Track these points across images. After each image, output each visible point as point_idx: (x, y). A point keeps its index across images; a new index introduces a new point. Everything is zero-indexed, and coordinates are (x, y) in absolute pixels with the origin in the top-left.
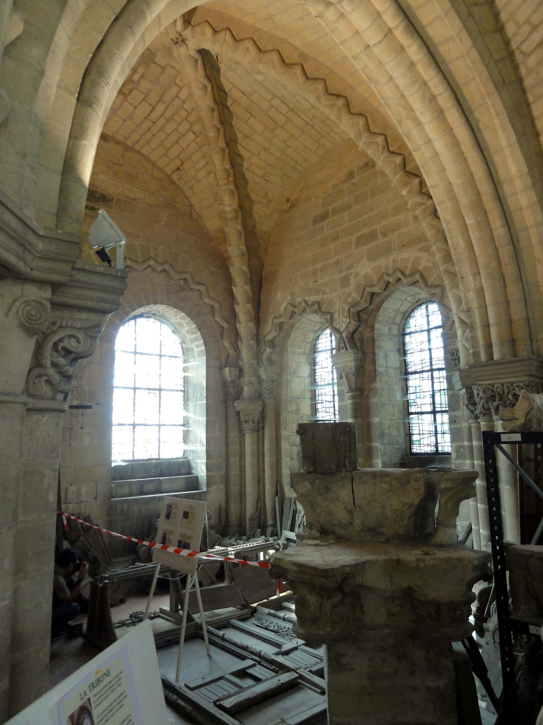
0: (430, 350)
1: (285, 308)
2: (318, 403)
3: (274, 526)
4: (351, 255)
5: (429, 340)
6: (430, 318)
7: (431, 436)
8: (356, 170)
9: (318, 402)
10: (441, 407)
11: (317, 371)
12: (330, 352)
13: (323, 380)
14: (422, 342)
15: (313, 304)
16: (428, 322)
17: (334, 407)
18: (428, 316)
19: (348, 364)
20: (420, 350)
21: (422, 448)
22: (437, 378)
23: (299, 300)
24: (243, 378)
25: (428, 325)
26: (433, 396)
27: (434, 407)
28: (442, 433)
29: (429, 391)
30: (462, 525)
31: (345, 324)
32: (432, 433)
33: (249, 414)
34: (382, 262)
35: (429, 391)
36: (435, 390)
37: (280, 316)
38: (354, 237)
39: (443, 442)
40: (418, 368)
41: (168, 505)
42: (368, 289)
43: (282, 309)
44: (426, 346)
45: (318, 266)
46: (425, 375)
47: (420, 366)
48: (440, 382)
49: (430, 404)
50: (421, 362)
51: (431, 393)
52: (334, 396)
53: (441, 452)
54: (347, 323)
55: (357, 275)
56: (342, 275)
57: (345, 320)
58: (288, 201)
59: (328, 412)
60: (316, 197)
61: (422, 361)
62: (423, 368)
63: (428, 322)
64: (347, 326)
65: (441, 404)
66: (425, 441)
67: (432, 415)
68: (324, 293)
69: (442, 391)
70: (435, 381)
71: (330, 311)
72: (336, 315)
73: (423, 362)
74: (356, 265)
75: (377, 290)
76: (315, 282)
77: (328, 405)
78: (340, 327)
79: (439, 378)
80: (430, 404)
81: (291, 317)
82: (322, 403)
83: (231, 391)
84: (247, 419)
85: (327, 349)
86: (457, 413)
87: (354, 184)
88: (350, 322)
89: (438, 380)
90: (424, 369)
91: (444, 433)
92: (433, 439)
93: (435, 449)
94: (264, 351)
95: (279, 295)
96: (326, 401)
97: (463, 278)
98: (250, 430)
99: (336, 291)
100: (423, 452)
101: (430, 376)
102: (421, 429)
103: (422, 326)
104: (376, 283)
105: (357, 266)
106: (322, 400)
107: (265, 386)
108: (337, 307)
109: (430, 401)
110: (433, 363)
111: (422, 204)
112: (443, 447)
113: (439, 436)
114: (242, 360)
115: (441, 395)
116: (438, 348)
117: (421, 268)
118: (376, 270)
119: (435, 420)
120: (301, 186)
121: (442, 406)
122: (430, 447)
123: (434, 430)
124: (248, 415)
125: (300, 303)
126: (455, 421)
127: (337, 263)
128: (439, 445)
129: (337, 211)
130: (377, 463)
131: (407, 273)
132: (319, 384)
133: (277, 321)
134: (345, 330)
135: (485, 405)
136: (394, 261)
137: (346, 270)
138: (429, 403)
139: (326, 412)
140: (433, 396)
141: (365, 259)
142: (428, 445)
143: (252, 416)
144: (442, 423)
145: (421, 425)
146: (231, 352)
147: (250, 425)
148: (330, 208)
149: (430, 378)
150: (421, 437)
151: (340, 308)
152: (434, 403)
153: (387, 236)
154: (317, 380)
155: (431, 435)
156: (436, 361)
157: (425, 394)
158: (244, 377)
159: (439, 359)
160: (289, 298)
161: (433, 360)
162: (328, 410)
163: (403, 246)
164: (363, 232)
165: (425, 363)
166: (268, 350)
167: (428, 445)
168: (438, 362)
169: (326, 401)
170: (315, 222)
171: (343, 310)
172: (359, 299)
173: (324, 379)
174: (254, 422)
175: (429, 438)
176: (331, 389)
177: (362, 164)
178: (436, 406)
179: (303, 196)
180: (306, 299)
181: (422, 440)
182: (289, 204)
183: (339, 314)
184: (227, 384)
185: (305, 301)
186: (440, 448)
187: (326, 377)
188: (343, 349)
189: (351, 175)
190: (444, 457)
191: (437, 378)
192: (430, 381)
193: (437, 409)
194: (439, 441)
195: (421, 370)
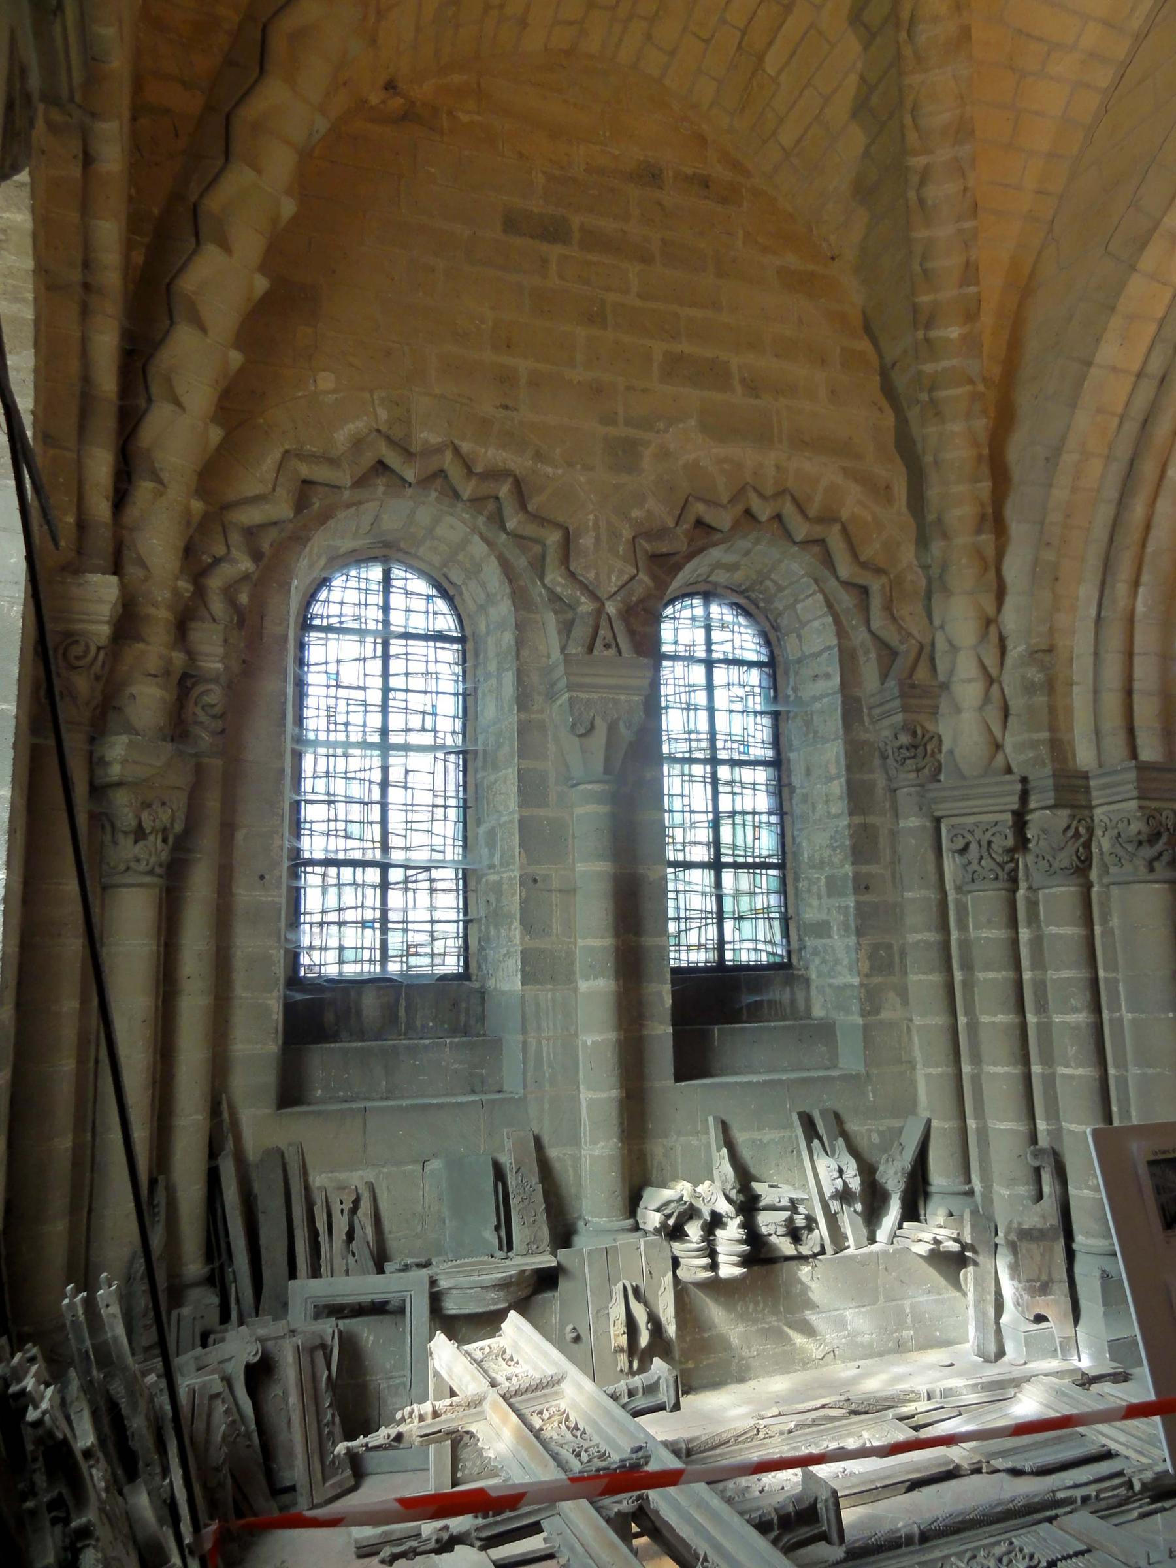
0: (711, 710)
1: (358, 444)
2: (312, 802)
3: (217, 1280)
4: (644, 391)
5: (710, 687)
6: (716, 635)
7: (707, 925)
8: (671, 174)
9: (310, 797)
10: (733, 855)
11: (311, 690)
12: (379, 640)
13: (341, 728)
14: (691, 688)
15: (494, 474)
16: (709, 642)
17: (384, 822)
18: (708, 629)
19: (623, 698)
20: (684, 706)
21: (684, 956)
22: (726, 783)
23: (427, 436)
24: (141, 646)
25: (709, 650)
26: (715, 825)
27: (718, 854)
28: (735, 919)
29: (706, 812)
30: (881, 1128)
31: (618, 578)
32: (710, 916)
33: (156, 806)
34: (748, 455)
35: (706, 812)
36: (720, 810)
37: (333, 462)
38: (659, 348)
39: (737, 938)
40: (681, 748)
41: (1151, 1163)
42: (700, 508)
43: (342, 436)
44: (701, 698)
45: (523, 365)
46: (697, 769)
47: (683, 747)
48: (734, 794)
49: (708, 845)
50: (686, 736)
51: (711, 816)
52: (385, 784)
53: (731, 963)
54: (626, 577)
55: (664, 454)
56: (612, 431)
57: (619, 564)
58: (390, 86)
59: (356, 834)
60: (521, 155)
61: (689, 732)
62: (690, 751)
63: (709, 642)
64: (622, 587)
65: (734, 847)
66: (693, 938)
67: (712, 872)
68: (539, 456)
69: (738, 817)
70: (721, 788)
71: (561, 519)
72: (587, 541)
73: (693, 736)
74: (661, 425)
75: (723, 519)
76: (506, 407)
77: (356, 812)
78: (597, 575)
79: (732, 783)
80: (708, 845)
81: (361, 482)
82: (329, 803)
83: (82, 684)
84: (147, 824)
85: (363, 626)
86: (873, 868)
87: (659, 204)
88: (632, 578)
89: (728, 789)
90: (695, 755)
91: (740, 918)
92: (712, 932)
93: (716, 958)
94: (217, 561)
95: (326, 381)
96: (349, 801)
97: (1057, 579)
98: (151, 872)
99: (588, 468)
100: (684, 964)
101: (709, 775)
102: (682, 906)
103: (692, 648)
104: (725, 501)
105: (666, 431)
106: (328, 794)
107: (212, 699)
108: (591, 517)
109: (703, 834)
110: (719, 744)
111: (971, 381)
112: (738, 952)
113: (728, 925)
114: (143, 564)
115: (734, 824)
116: (731, 711)
117: (845, 515)
118: (726, 466)
119: (718, 884)
120: (457, 79)
121: (737, 852)
122: (703, 952)
123: (715, 910)
124: (149, 806)
125: (431, 451)
126: (867, 888)
127: (597, 390)
128: (726, 946)
129: (593, 240)
130: (660, 994)
131: (812, 512)
132: (322, 736)
133: (305, 470)
134: (616, 592)
135: (1081, 850)
136: (778, 467)
137: (627, 423)
138: (705, 840)
139: (347, 837)
140: (715, 825)
141: (693, 423)
142: (699, 947)
143: (164, 816)
144: (737, 894)
145: (682, 896)
146: (101, 507)
147: (154, 851)
148: (576, 220)
149: (708, 780)
150: (683, 927)
151: (603, 524)
152: (716, 843)
153: (757, 397)
154: (310, 724)
155: (709, 921)
156: (726, 741)
157: (698, 817)
158: (139, 638)
159: (734, 738)
160: (383, 414)
161: (718, 737)
162: (355, 829)
163: (802, 442)
164: (684, 347)
165: (698, 740)
166: (246, 565)
167: (699, 947)
168: (729, 745)
169: (349, 801)
170: (512, 223)
171: (614, 534)
172: (671, 523)
173: (347, 724)
174: (165, 841)
175: (703, 928)
176: (377, 762)
177: (689, 171)
178: (723, 851)
179: (464, 118)
180: (466, 447)
181: (683, 934)
182: (396, 103)
183: (598, 539)
184: (77, 650)
185: (456, 451)
186: (729, 955)
187: (356, 718)
188: (607, 646)
189: (651, 176)
190: (759, 975)
191: (726, 783)
192: (709, 788)
193: (724, 859)
194: (728, 937)
195: (687, 755)
